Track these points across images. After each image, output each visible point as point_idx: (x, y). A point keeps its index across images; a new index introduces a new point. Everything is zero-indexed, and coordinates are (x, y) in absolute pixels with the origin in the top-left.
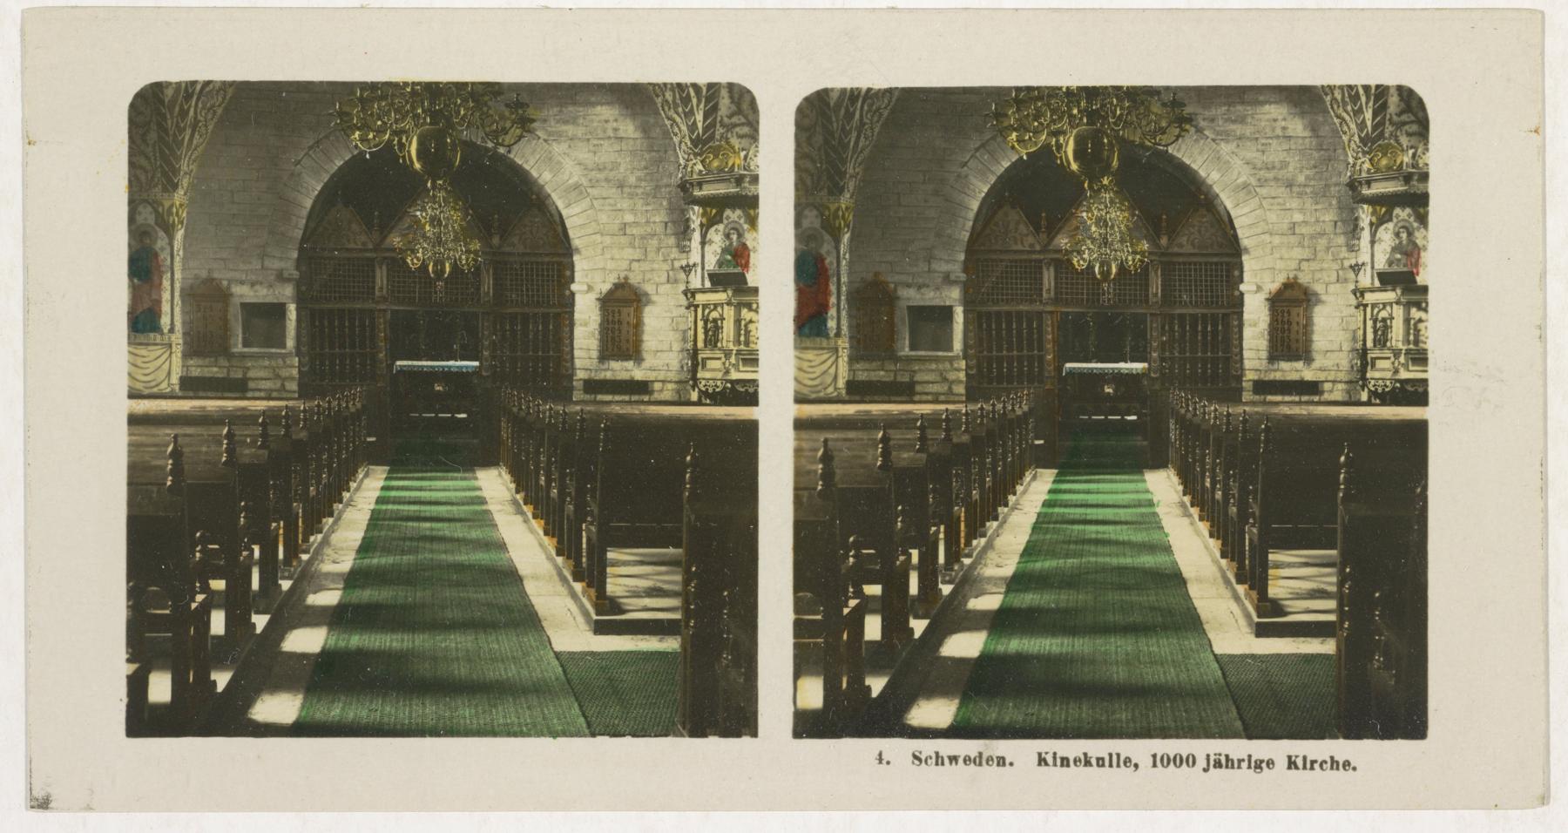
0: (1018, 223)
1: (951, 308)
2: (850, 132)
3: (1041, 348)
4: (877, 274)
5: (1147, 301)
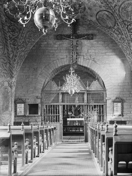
0: (53, 84)
1: (37, 105)
3: (59, 114)
5: (84, 102)
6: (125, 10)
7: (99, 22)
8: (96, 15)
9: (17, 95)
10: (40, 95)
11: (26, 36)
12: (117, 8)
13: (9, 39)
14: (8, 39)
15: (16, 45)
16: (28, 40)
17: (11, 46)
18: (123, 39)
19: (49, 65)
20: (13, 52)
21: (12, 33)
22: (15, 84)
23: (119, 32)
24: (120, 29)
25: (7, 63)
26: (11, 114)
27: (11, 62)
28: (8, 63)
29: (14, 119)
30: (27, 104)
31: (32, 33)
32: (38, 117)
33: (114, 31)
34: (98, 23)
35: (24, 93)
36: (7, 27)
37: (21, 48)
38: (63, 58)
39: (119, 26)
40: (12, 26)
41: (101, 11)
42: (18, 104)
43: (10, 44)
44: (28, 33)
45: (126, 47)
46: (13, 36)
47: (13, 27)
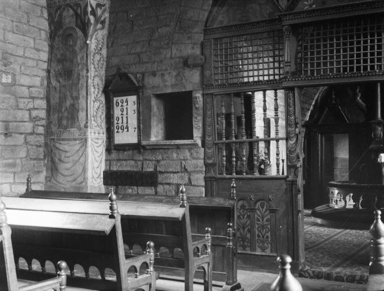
1: (190, 93)
9: (115, 61)
10: (198, 51)
22: (107, 15)
26: (86, 140)
30: (149, 92)
32: (190, 150)
35: (138, 50)
42: (115, 99)
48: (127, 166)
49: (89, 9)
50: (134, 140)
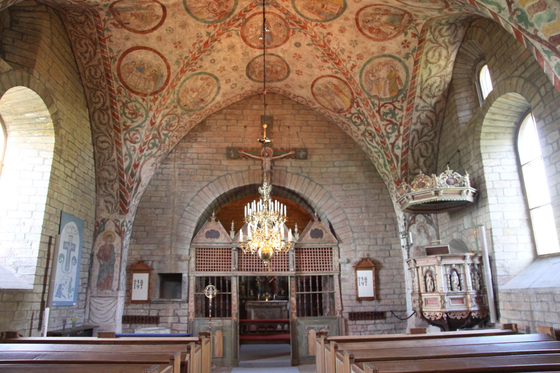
1: (180, 275)
2: (133, 183)
4: (141, 256)
5: (288, 270)
6: (372, 76)
7: (316, 99)
8: (312, 86)
11: (161, 124)
12: (356, 70)
13: (124, 130)
14: (122, 129)
15: (139, 142)
16: (165, 132)
17: (125, 144)
18: (370, 134)
19: (209, 187)
20: (131, 157)
21: (130, 116)
22: (131, 227)
23: (361, 119)
24: (363, 114)
25: (115, 180)
27: (125, 178)
28: (117, 181)
29: (124, 309)
30: (155, 272)
31: (174, 119)
32: (180, 304)
33: (351, 117)
34: (314, 101)
36: (121, 104)
37: (149, 148)
38: (242, 172)
39: (361, 107)
40: (131, 101)
41: (323, 77)
43: (125, 140)
44: (166, 119)
45: (376, 150)
46: (133, 122)
47: (133, 104)
48: (141, 312)
49: (125, 224)
50: (146, 298)
